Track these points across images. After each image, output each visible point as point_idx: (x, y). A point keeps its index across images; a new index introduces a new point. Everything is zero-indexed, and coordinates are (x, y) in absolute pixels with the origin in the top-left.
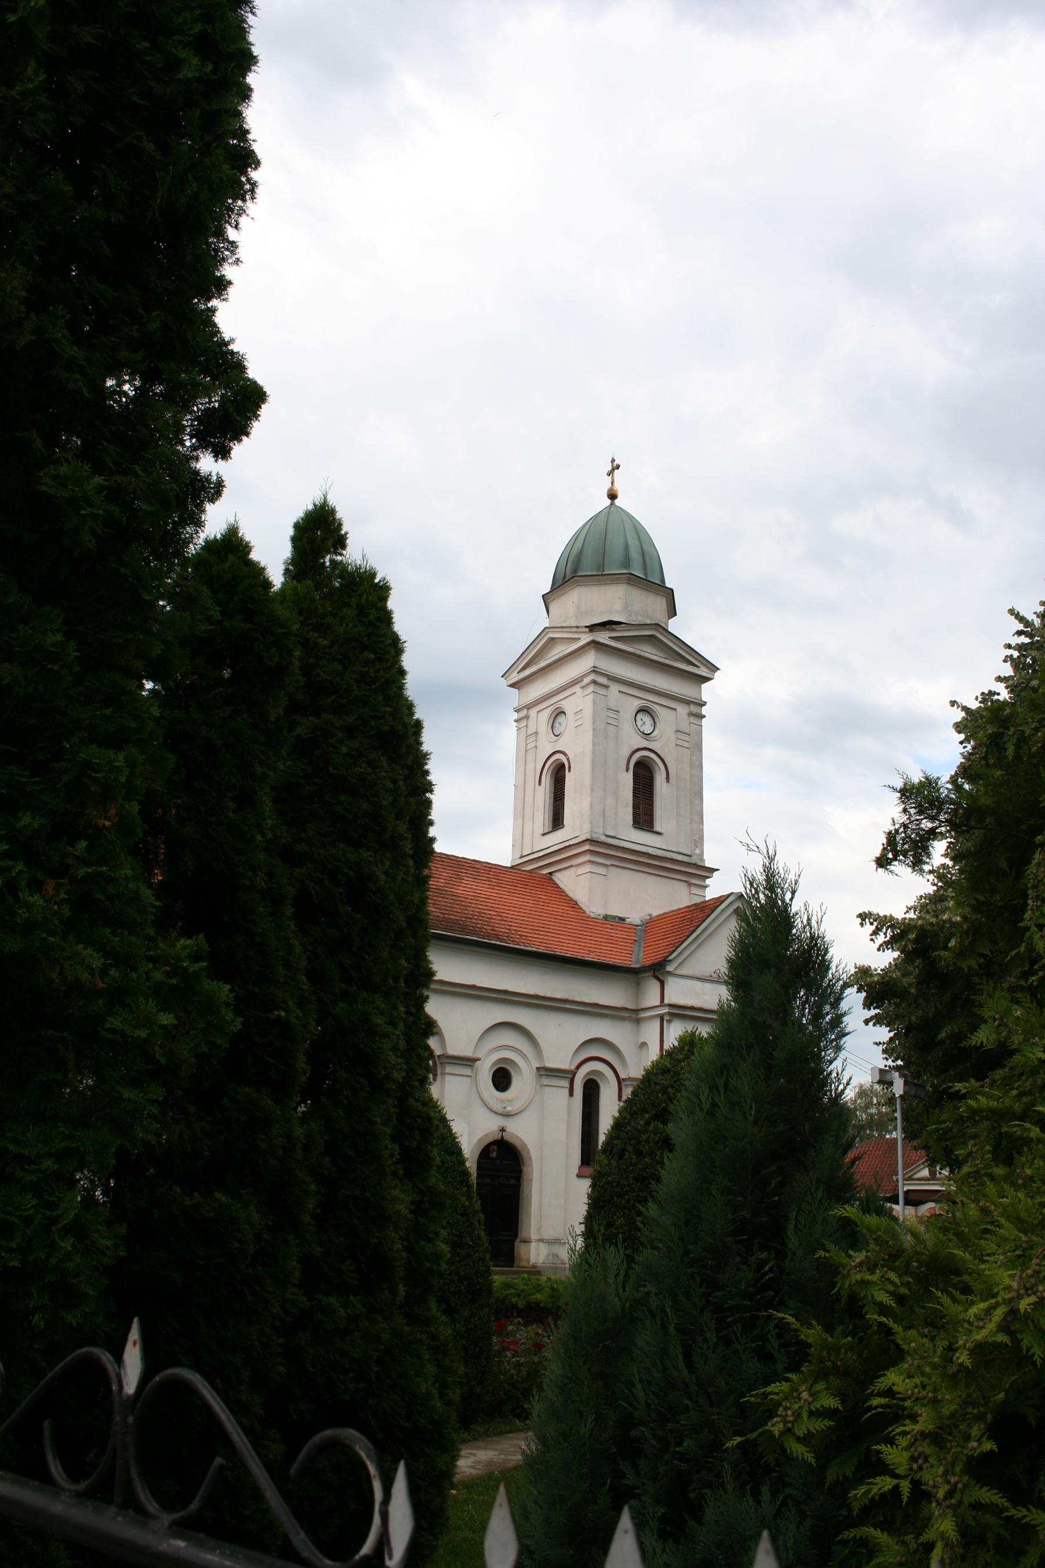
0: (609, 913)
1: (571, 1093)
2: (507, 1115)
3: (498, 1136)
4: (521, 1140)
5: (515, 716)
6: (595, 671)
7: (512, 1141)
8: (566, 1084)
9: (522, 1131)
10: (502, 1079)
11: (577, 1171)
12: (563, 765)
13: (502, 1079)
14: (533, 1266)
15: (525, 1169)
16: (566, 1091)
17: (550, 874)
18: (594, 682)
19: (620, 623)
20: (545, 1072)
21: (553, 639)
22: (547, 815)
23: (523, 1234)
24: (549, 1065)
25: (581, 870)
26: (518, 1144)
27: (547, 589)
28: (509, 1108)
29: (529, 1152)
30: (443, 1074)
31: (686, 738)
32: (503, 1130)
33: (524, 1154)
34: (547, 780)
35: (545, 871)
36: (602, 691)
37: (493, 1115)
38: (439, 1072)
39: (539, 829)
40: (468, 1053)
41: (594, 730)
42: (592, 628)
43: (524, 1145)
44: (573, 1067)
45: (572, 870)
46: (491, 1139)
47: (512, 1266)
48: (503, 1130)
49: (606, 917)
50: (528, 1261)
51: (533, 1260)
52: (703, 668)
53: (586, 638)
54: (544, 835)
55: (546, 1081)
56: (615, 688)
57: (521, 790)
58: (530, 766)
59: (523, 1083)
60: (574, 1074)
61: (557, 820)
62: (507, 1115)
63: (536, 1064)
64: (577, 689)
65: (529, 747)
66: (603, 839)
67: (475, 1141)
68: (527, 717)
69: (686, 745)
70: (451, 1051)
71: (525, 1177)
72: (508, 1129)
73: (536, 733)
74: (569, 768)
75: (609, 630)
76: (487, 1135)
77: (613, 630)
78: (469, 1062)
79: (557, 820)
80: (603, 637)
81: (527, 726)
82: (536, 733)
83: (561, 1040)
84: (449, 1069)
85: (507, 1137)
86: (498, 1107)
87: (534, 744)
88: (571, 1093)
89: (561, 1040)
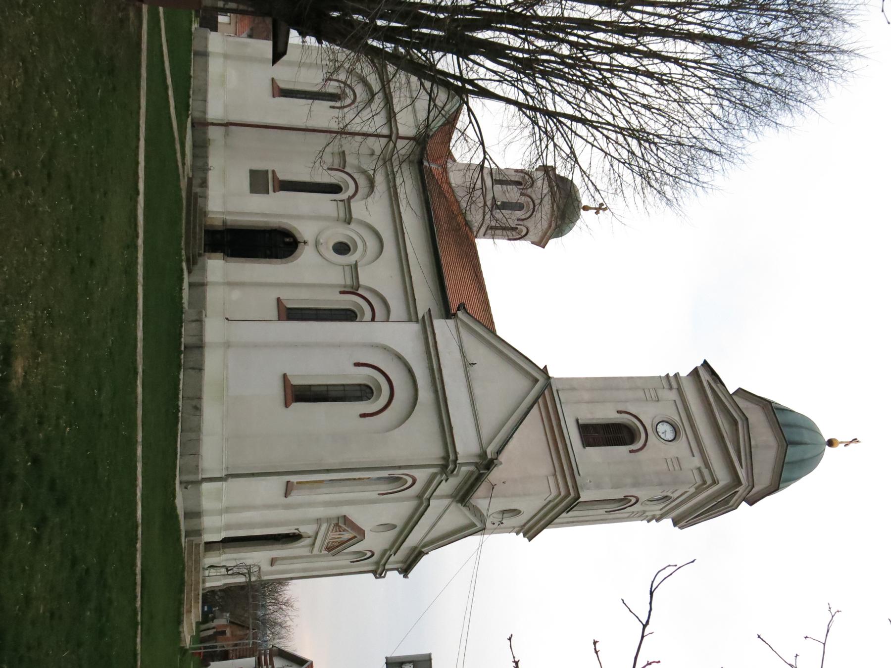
9: (306, 255)
10: (342, 248)
20: (355, 268)
31: (677, 468)
32: (305, 243)
33: (291, 258)
40: (354, 216)
43: (296, 259)
46: (297, 236)
50: (209, 258)
62: (317, 244)
69: (671, 468)
72: (306, 247)
77: (715, 382)
85: (300, 246)
89: (380, 276)
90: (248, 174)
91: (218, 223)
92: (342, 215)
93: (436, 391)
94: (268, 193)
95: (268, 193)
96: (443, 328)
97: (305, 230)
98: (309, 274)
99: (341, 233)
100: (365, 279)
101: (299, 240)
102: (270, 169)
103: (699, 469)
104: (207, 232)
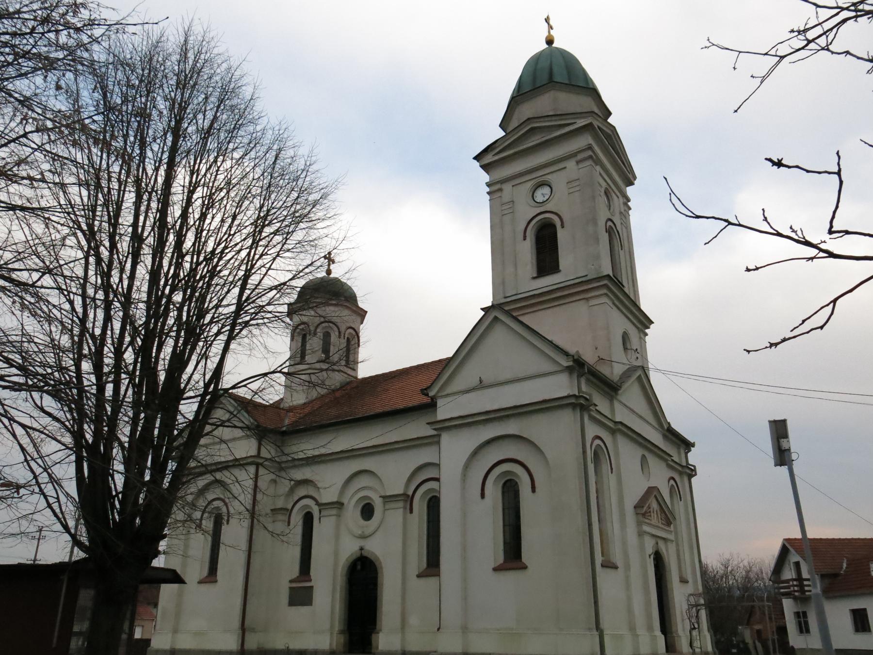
7: (369, 556)
9: (375, 548)
10: (367, 511)
20: (387, 499)
26: (372, 558)
32: (362, 549)
33: (377, 564)
40: (335, 500)
46: (354, 557)
50: (377, 648)
52: (578, 121)
62: (363, 537)
69: (577, 189)
71: (379, 582)
77: (495, 148)
83: (395, 472)
85: (365, 554)
89: (395, 472)
90: (294, 608)
92: (334, 512)
93: (508, 416)
94: (312, 587)
95: (312, 587)
96: (445, 410)
97: (349, 548)
98: (393, 544)
99: (352, 513)
101: (359, 555)
102: (289, 585)
103: (578, 162)
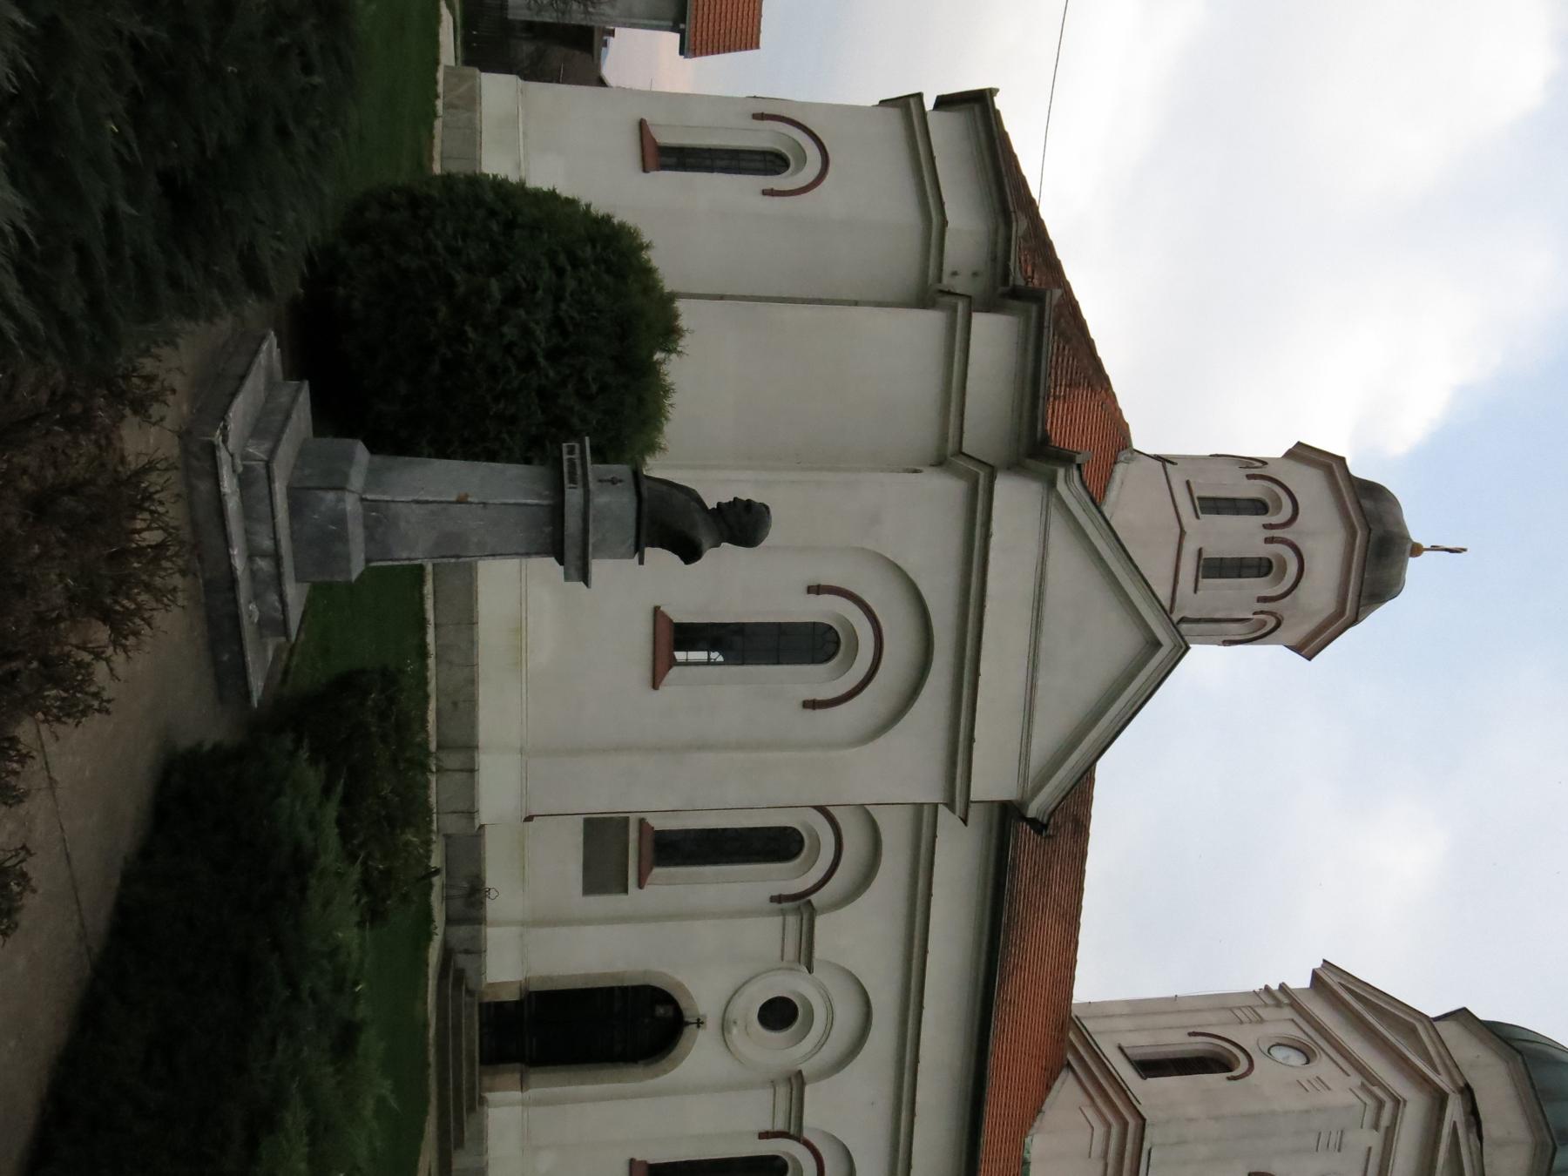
0: (1032, 1168)
1: (764, 1135)
2: (724, 1027)
3: (689, 1016)
4: (687, 1054)
5: (1275, 987)
6: (1398, 1102)
7: (683, 1042)
8: (780, 1126)
9: (700, 1055)
10: (779, 1014)
11: (638, 1158)
12: (1230, 1070)
13: (779, 1014)
14: (483, 1101)
15: (638, 1070)
16: (768, 1127)
17: (1069, 1065)
18: (1380, 1105)
19: (1480, 1138)
20: (797, 1082)
21: (1414, 1031)
22: (1149, 1050)
23: (535, 1076)
24: (808, 1089)
25: (1090, 1113)
27: (1483, 1014)
28: (735, 1031)
29: (665, 1072)
30: (783, 913)
33: (664, 1063)
34: (1199, 1045)
35: (1070, 1057)
36: (1369, 1118)
37: (724, 1003)
38: (785, 905)
39: (1129, 1041)
40: (818, 953)
41: (1307, 1112)
42: (1467, 1092)
43: (675, 1064)
44: (806, 1135)
45: (1087, 1101)
46: (683, 1004)
47: (482, 1062)
48: (699, 1023)
49: (1026, 1163)
50: (491, 1090)
51: (489, 1096)
53: (1442, 1081)
54: (1121, 1049)
55: (783, 1091)
56: (1374, 1139)
57: (1173, 1005)
58: (1212, 1017)
59: (776, 1051)
60: (798, 1138)
61: (1150, 1067)
62: (724, 1027)
63: (806, 1069)
64: (1356, 1080)
65: (1239, 1013)
66: (1146, 1145)
67: (679, 978)
68: (1279, 1004)
70: (820, 921)
73: (1261, 1021)
74: (1235, 1078)
75: (1467, 1121)
76: (690, 997)
77: (1468, 1127)
78: (806, 956)
79: (1150, 1067)
80: (1454, 1111)
81: (1266, 1005)
82: (1261, 1021)
84: (792, 921)
85: (688, 1031)
86: (736, 1011)
87: (1244, 1018)
88: (764, 1135)
91: (510, 996)
95: (626, 891)
97: (703, 994)
100: (813, 1120)
104: (486, 1008)
